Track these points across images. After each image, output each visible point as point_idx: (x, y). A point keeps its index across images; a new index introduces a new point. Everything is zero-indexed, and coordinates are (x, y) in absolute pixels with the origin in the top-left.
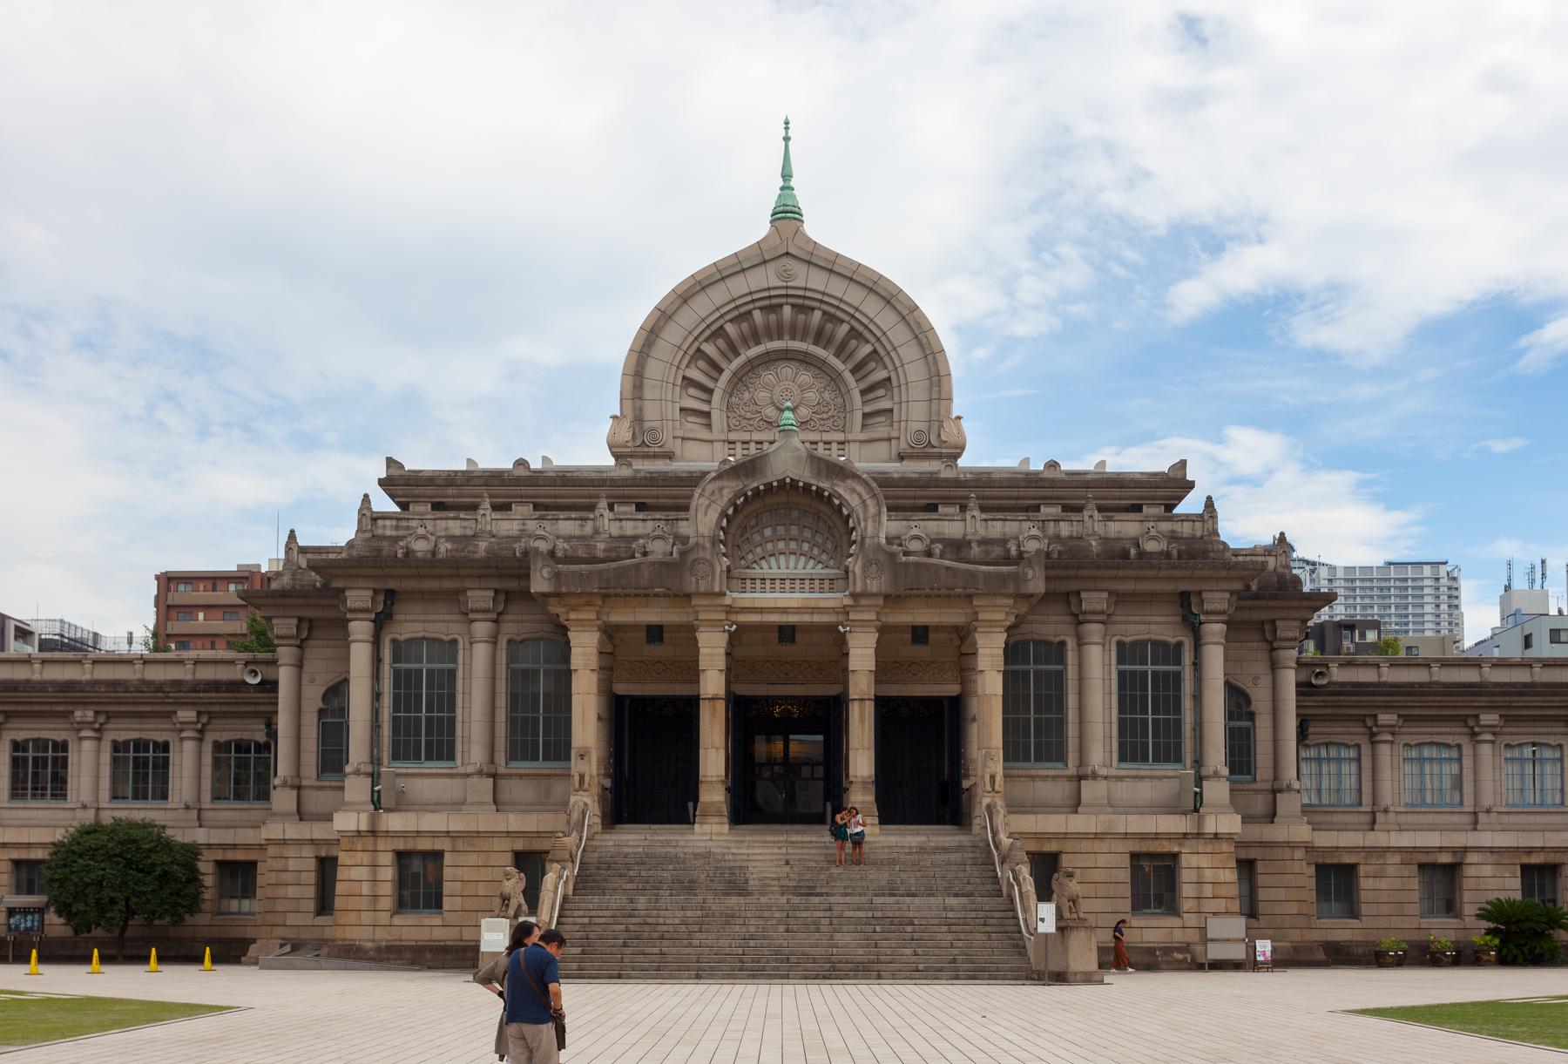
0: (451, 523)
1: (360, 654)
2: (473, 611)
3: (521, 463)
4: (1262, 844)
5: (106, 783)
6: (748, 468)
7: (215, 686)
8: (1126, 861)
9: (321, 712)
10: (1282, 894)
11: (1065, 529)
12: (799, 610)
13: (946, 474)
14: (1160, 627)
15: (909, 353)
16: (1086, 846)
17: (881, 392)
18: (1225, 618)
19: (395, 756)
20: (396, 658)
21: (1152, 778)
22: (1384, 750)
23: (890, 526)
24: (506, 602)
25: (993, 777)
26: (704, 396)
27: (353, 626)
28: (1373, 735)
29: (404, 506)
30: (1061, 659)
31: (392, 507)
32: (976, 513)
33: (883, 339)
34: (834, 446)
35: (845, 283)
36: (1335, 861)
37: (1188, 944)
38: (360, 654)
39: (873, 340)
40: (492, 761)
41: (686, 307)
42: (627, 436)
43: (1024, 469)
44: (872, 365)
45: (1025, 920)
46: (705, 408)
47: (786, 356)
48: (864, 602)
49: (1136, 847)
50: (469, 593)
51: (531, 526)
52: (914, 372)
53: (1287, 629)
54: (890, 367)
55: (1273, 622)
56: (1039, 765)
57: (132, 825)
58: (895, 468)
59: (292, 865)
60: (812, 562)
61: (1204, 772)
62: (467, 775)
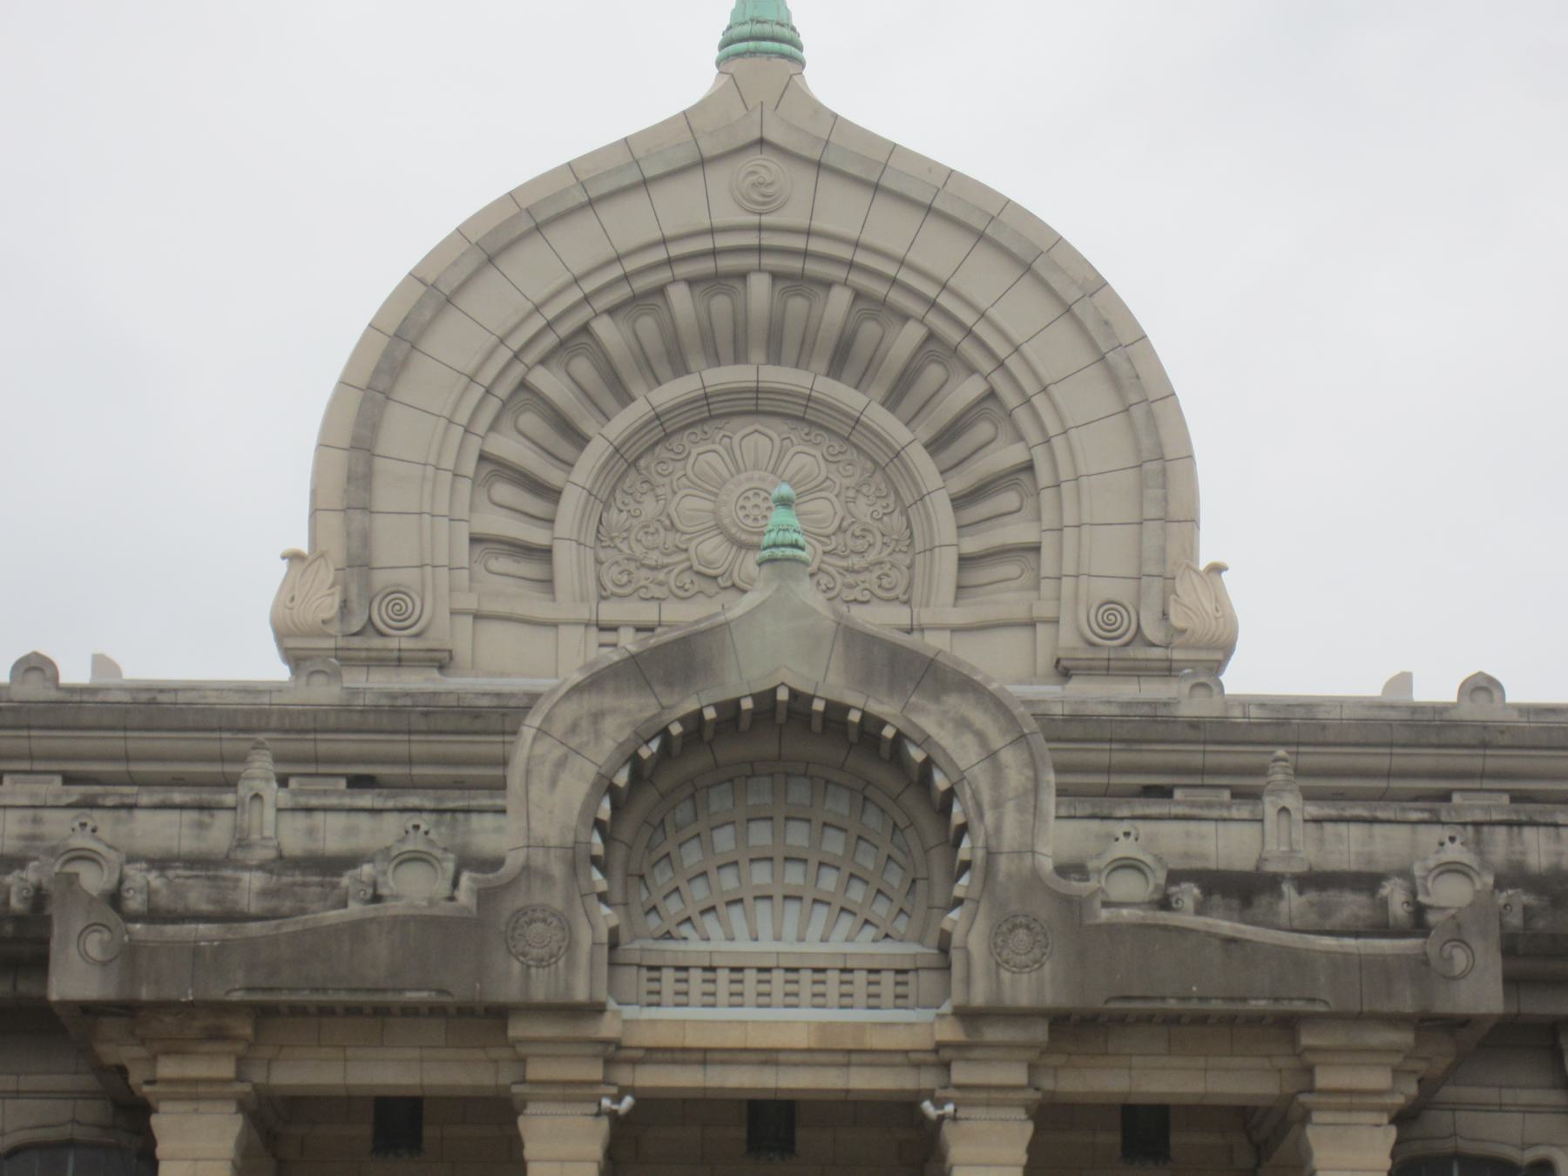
6: (677, 659)
13: (1193, 707)
15: (1083, 398)
17: (1007, 500)
23: (1062, 837)
26: (536, 505)
32: (1291, 801)
33: (1013, 363)
35: (912, 219)
39: (985, 365)
41: (492, 275)
42: (328, 606)
43: (1398, 698)
44: (983, 430)
47: (756, 405)
48: (993, 1034)
51: (60, 826)
52: (1099, 450)
54: (1033, 436)
58: (1058, 697)
60: (846, 922)
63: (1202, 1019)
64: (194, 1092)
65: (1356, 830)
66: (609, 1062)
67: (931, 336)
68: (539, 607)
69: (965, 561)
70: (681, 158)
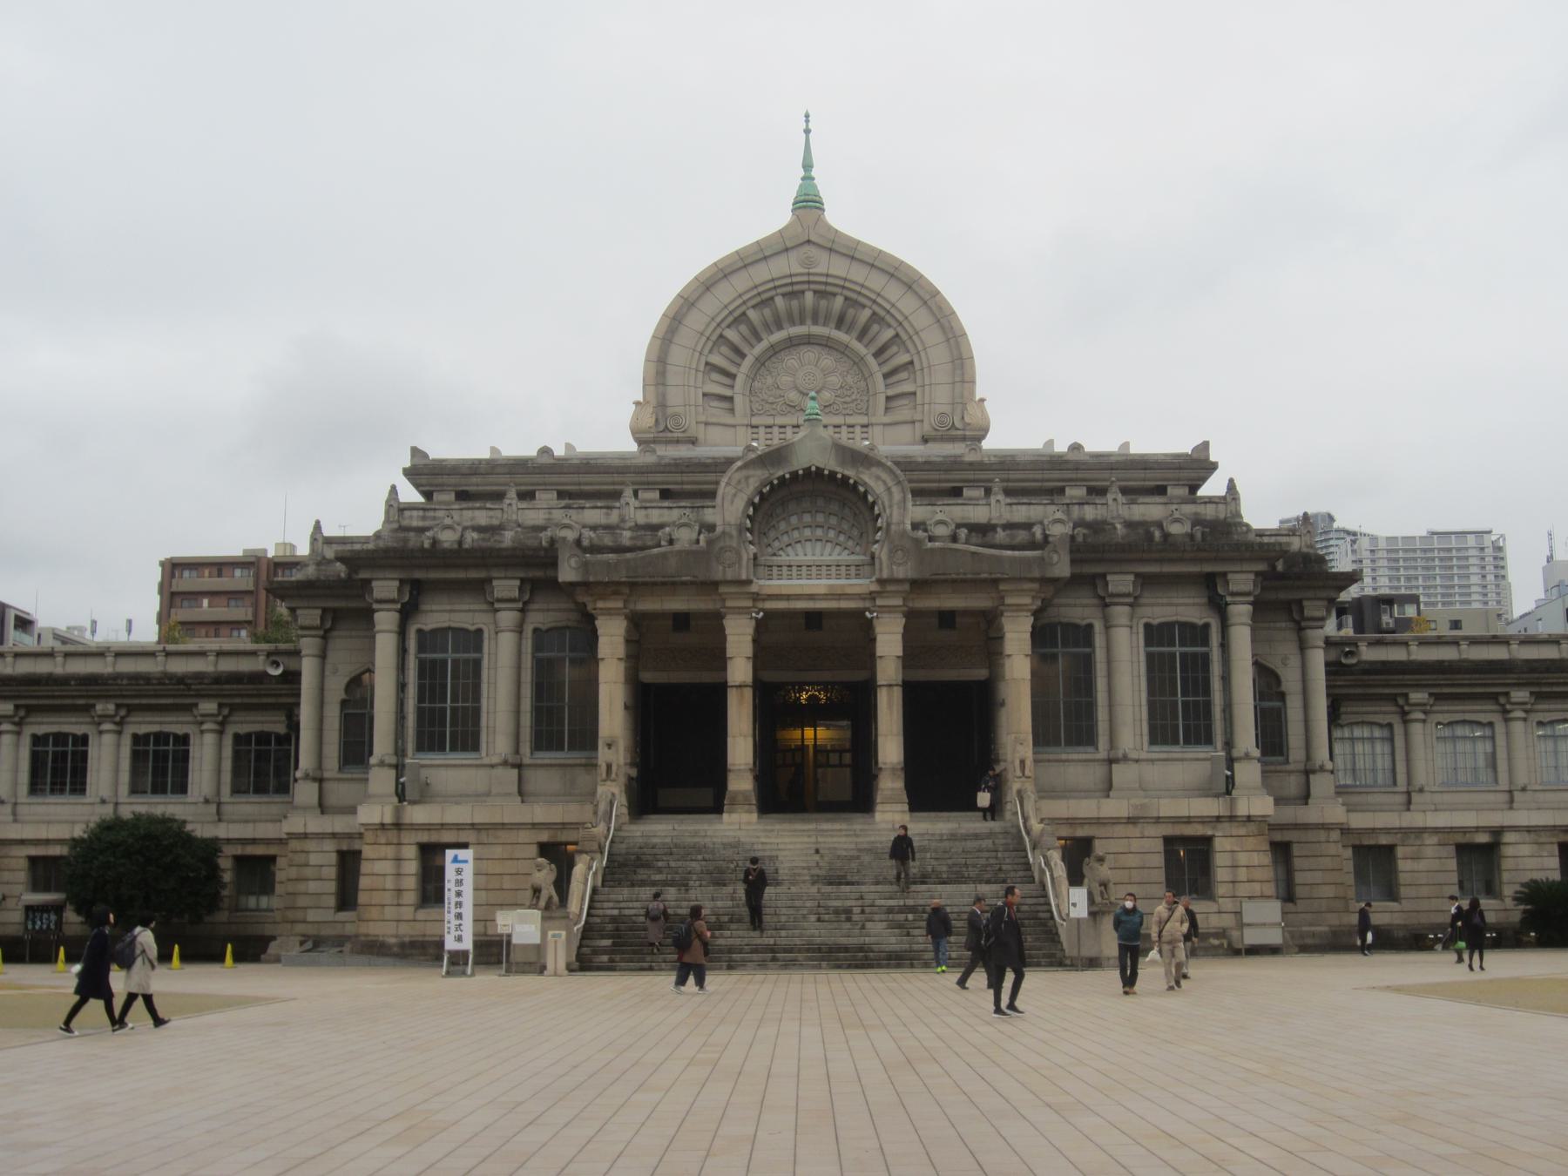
0: (477, 513)
1: (385, 646)
2: (499, 600)
3: (545, 451)
4: (1297, 827)
5: (125, 777)
6: (774, 457)
7: (236, 678)
8: (1159, 846)
9: (344, 703)
10: (1318, 877)
11: (1090, 513)
12: (826, 597)
13: (971, 457)
14: (1187, 608)
15: (932, 337)
16: (1120, 830)
17: (904, 375)
18: (1251, 599)
19: (420, 748)
20: (421, 648)
21: (1182, 760)
22: (1416, 729)
23: (918, 512)
24: (532, 592)
25: (1022, 762)
27: (377, 616)
28: (1404, 714)
29: (428, 495)
30: (1089, 642)
31: (418, 498)
32: (1001, 497)
34: (858, 429)
36: (1372, 842)
37: (1224, 930)
38: (385, 646)
40: (517, 752)
43: (1048, 451)
44: (894, 349)
45: (1058, 906)
46: (728, 393)
47: (809, 340)
48: (890, 588)
49: (1170, 830)
50: (495, 583)
51: (558, 515)
52: (937, 355)
53: (1312, 609)
55: (1300, 602)
56: (1069, 749)
57: (152, 820)
58: (919, 451)
59: (314, 859)
60: (838, 549)
61: (1235, 754)
62: (492, 766)
63: (964, 581)
64: (609, 612)
65: (1024, 508)
66: (754, 600)
67: (874, 313)
68: (729, 420)
69: (888, 399)
70: (780, 247)
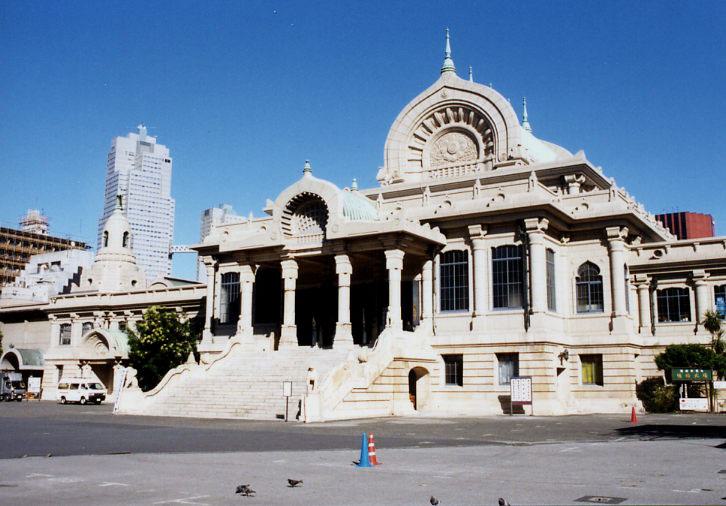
14: (507, 239)
